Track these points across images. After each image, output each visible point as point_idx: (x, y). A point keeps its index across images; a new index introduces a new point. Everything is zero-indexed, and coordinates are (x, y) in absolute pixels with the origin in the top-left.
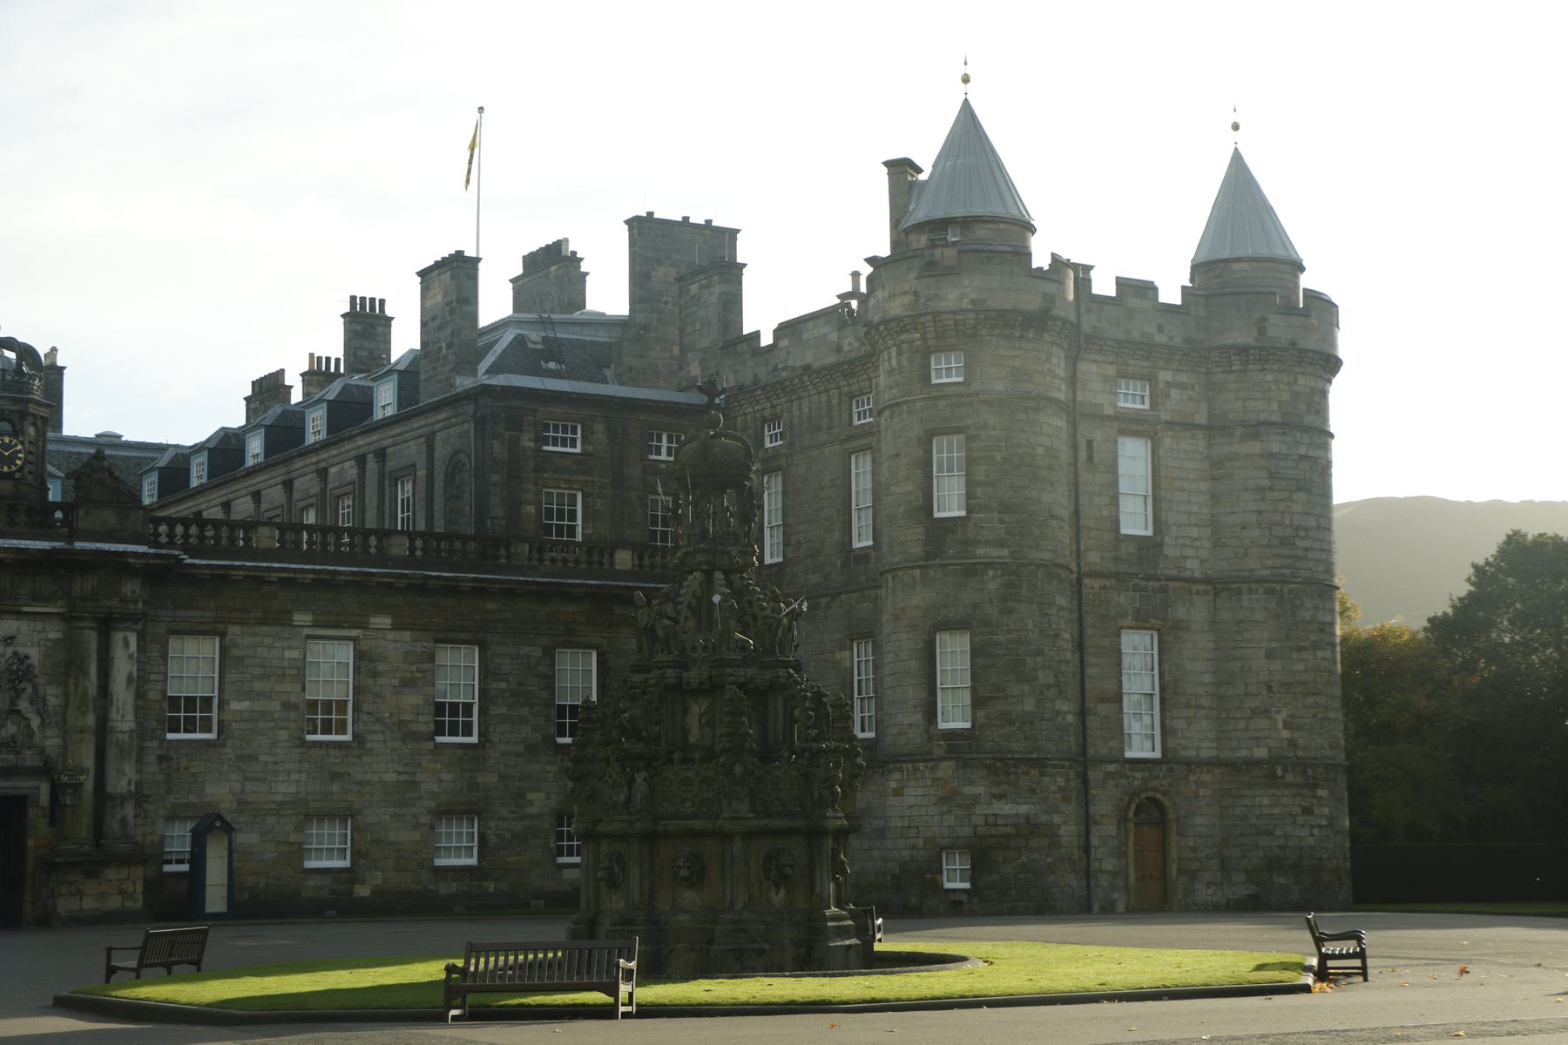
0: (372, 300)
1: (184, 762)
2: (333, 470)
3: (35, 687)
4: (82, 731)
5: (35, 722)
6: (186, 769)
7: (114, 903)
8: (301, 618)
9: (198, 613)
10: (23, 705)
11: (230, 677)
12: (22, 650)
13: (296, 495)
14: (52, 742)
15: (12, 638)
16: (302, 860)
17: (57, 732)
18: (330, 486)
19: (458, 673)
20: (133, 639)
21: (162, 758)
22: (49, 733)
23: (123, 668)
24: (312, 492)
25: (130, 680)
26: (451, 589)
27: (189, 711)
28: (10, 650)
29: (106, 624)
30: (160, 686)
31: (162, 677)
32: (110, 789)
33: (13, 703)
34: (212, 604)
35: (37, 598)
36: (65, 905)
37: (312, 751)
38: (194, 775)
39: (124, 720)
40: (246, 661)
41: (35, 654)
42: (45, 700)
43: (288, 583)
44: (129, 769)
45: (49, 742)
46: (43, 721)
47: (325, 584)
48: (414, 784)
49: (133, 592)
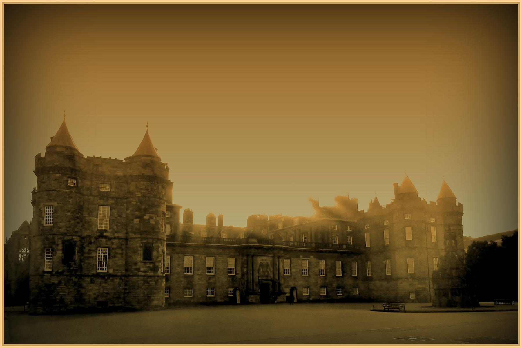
7: (282, 300)
8: (301, 256)
10: (268, 270)
11: (292, 265)
19: (322, 265)
23: (281, 264)
26: (322, 252)
27: (286, 271)
29: (279, 257)
35: (269, 254)
41: (269, 263)
43: (300, 251)
47: (305, 251)
48: (317, 282)
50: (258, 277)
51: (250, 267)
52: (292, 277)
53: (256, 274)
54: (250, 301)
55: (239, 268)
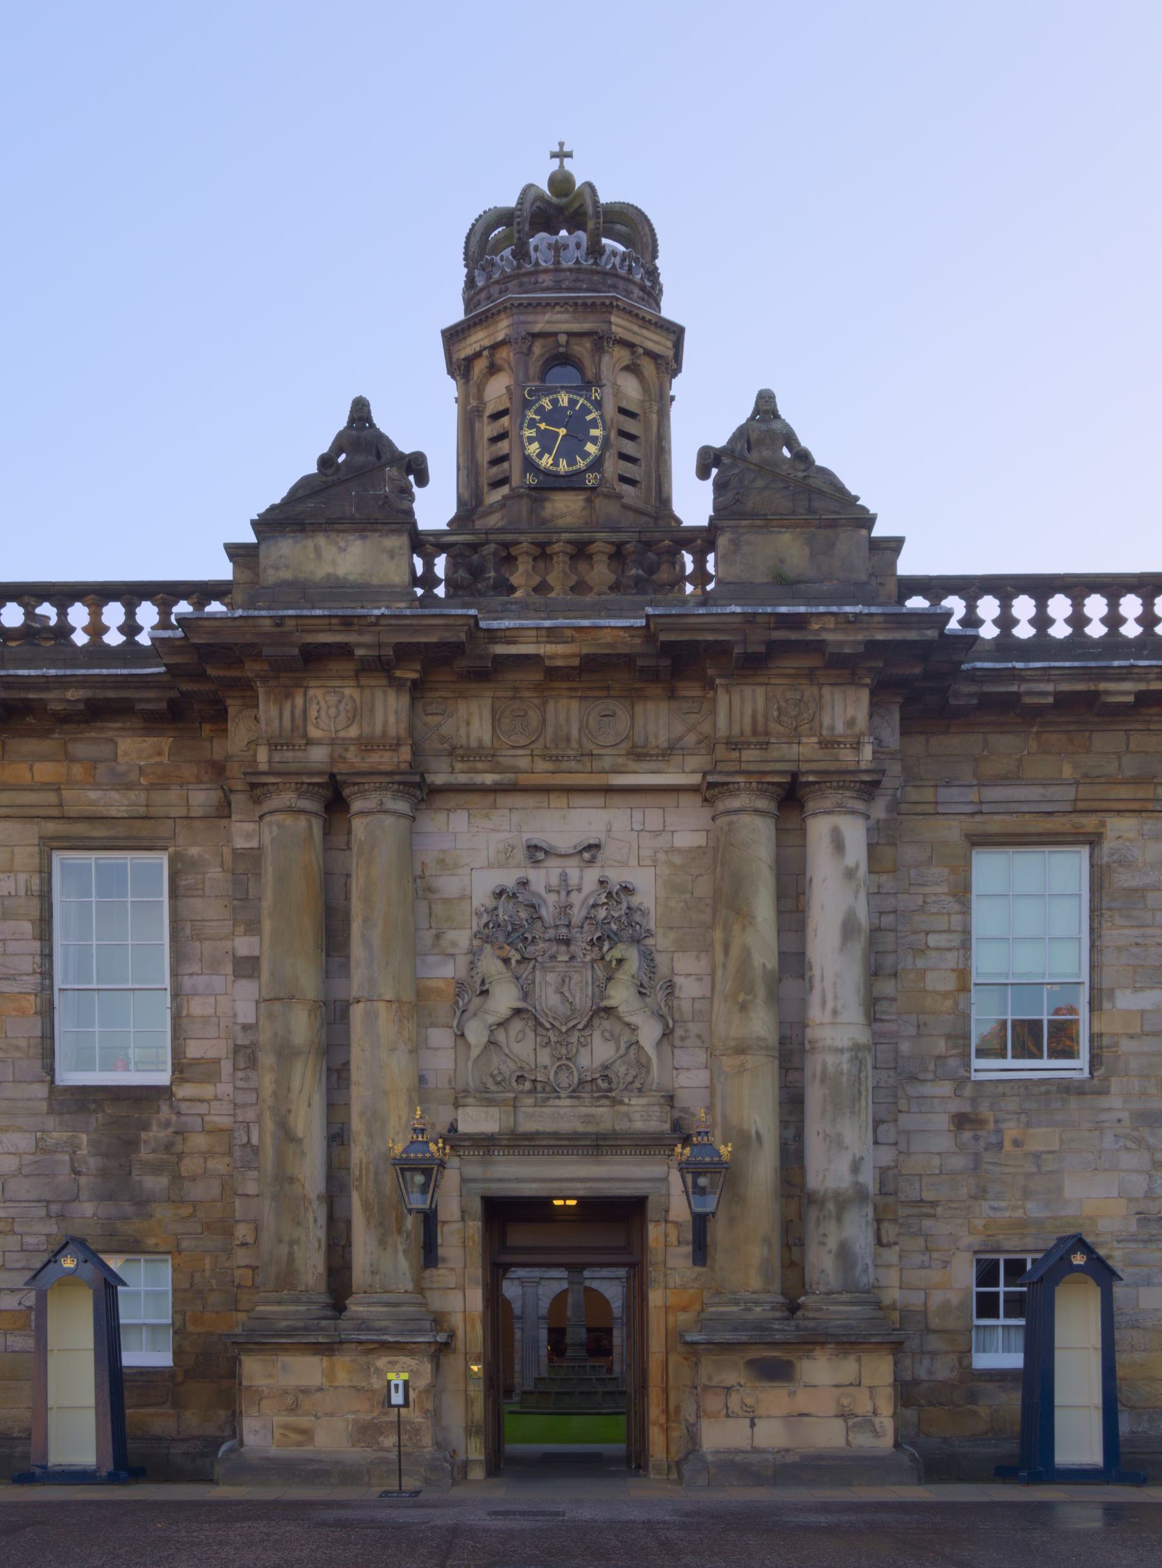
1: (1011, 1130)
3: (648, 957)
4: (741, 1050)
5: (649, 1034)
6: (1016, 1143)
10: (621, 995)
11: (1116, 934)
12: (616, 877)
14: (690, 1080)
15: (594, 847)
17: (702, 1057)
20: (855, 833)
21: (961, 1121)
22: (682, 1057)
25: (849, 928)
28: (592, 876)
30: (952, 960)
31: (956, 940)
32: (813, 1181)
35: (639, 754)
38: (1037, 1156)
39: (837, 1020)
41: (647, 887)
42: (670, 986)
44: (854, 1134)
45: (684, 1079)
46: (667, 1034)
52: (1116, 1103)
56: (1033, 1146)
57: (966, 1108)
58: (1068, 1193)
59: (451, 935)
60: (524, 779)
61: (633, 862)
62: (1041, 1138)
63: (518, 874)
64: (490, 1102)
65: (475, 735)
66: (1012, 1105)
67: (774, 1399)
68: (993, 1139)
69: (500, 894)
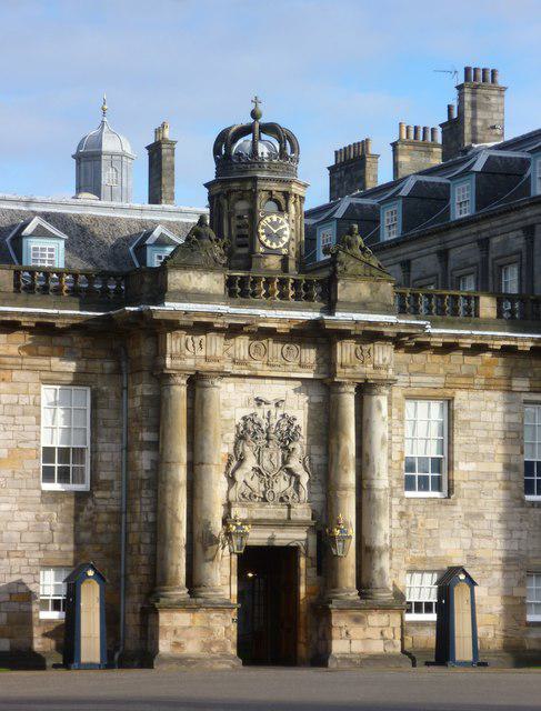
0: (484, 71)
1: (421, 519)
2: (495, 241)
7: (377, 647)
9: (429, 379)
10: (295, 464)
11: (458, 439)
12: (290, 414)
13: (451, 265)
16: (524, 613)
18: (492, 256)
20: (384, 401)
21: (402, 514)
23: (380, 428)
24: (471, 261)
29: (364, 390)
33: (285, 462)
34: (442, 370)
36: (339, 646)
37: (532, 510)
40: (472, 425)
49: (384, 360)
50: (228, 505)
51: (180, 451)
52: (459, 509)
53: (217, 489)
54: (164, 646)
55: (110, 452)
56: (429, 527)
57: (404, 510)
58: (442, 546)
59: (227, 435)
60: (260, 373)
61: (296, 408)
62: (432, 523)
63: (253, 411)
64: (243, 506)
65: (242, 354)
66: (420, 509)
67: (356, 631)
68: (414, 523)
69: (244, 418)
